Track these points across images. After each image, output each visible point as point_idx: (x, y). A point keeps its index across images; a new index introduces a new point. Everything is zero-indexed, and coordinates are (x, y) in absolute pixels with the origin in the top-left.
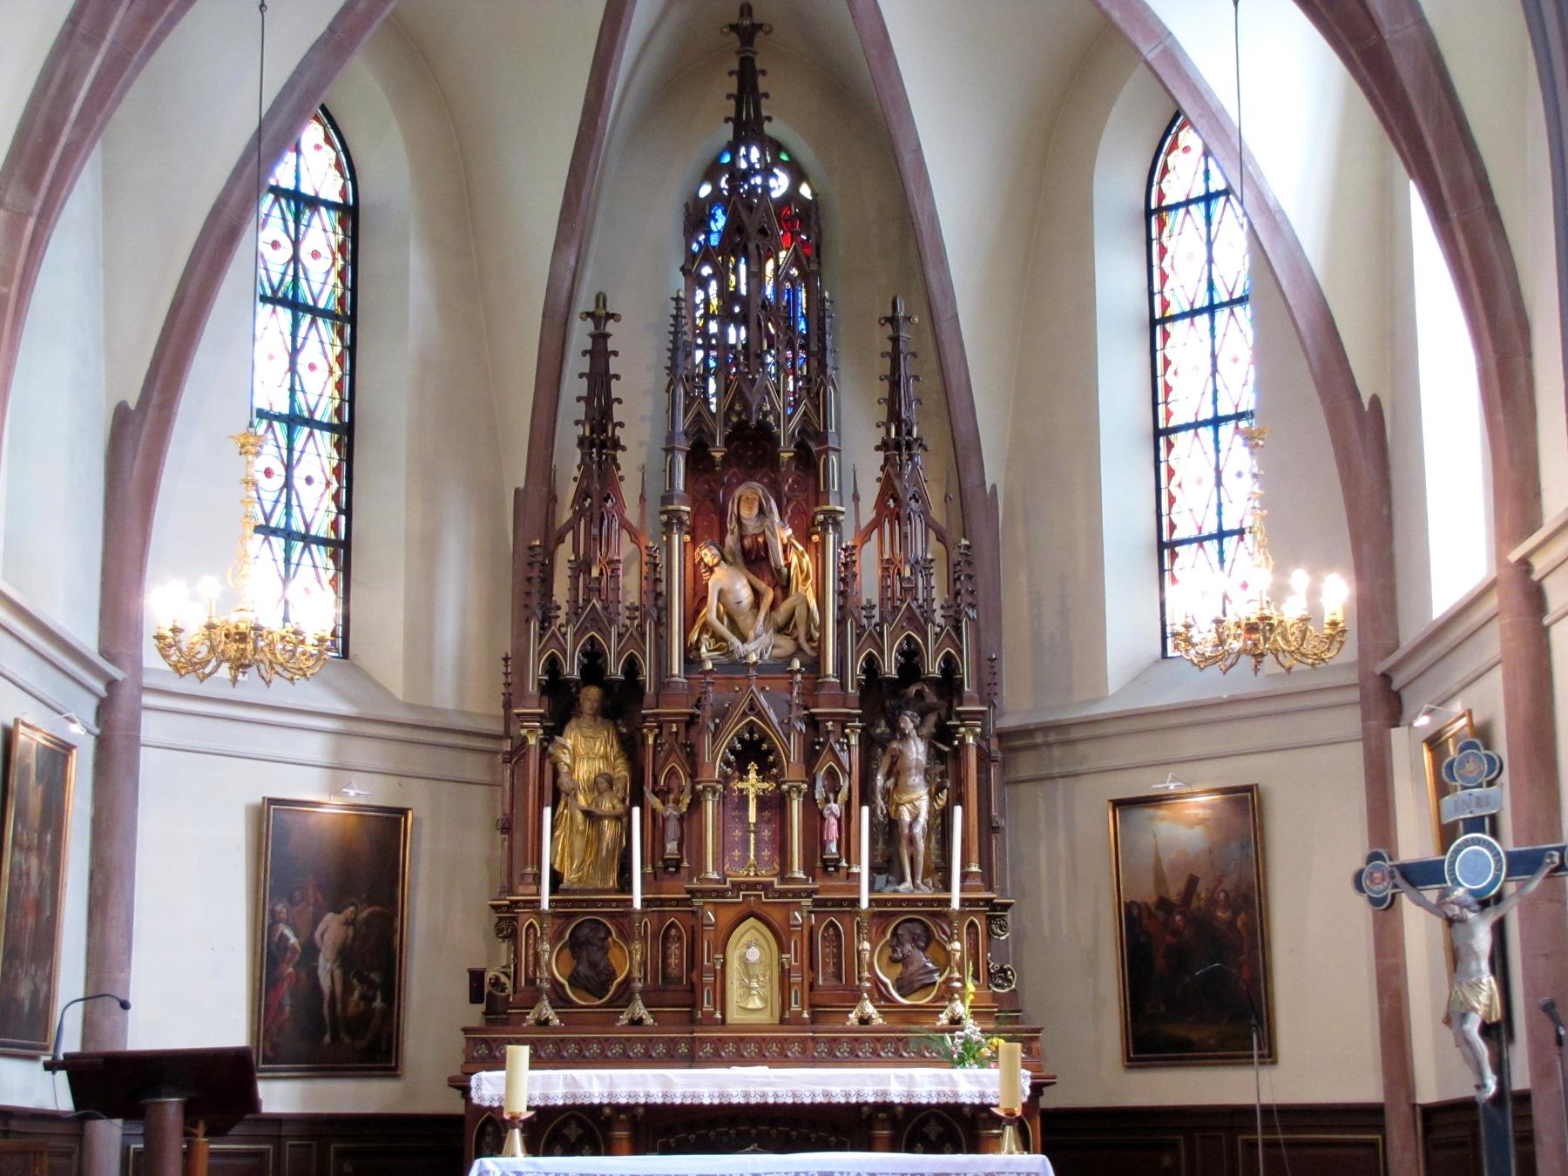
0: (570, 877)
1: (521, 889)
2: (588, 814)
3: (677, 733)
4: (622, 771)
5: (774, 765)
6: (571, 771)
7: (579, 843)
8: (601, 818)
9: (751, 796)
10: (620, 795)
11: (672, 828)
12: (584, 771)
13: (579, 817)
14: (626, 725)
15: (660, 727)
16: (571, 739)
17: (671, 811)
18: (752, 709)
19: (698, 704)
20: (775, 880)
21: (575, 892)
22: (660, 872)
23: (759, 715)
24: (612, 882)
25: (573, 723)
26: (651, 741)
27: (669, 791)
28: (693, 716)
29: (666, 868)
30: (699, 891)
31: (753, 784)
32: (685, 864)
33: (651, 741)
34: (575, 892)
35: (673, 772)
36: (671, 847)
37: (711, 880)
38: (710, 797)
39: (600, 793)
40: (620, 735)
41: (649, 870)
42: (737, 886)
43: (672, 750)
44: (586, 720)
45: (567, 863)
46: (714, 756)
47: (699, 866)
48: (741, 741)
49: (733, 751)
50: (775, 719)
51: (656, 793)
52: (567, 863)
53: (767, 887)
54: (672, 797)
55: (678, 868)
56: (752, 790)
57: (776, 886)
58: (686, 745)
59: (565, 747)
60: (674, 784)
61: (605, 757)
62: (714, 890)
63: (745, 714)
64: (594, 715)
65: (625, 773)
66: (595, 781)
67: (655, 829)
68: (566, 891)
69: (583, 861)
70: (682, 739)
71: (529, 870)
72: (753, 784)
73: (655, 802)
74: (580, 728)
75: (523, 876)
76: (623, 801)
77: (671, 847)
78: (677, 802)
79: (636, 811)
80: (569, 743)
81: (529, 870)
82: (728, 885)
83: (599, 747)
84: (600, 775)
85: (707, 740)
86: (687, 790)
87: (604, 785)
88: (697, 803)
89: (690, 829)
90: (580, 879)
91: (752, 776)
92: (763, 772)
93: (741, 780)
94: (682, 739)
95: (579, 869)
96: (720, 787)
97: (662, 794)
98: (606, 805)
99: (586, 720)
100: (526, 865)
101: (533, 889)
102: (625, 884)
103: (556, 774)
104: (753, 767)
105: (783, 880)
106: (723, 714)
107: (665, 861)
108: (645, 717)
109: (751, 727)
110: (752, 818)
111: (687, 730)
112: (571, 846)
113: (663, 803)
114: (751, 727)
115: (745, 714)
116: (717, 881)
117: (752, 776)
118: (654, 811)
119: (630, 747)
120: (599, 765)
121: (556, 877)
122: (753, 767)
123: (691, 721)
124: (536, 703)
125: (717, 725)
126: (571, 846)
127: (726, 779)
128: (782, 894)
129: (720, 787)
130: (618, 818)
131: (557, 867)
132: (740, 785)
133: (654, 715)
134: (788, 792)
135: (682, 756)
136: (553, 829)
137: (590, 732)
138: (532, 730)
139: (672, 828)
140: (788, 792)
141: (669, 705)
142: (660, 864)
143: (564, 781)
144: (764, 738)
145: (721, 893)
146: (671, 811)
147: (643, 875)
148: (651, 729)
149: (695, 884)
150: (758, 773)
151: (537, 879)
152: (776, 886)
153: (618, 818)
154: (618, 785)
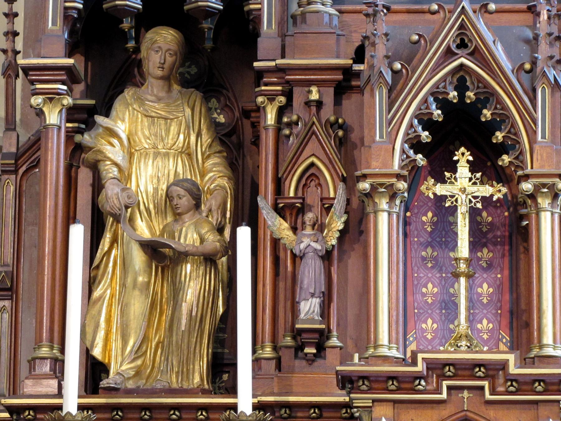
0: (120, 367)
1: (29, 386)
2: (153, 249)
3: (319, 104)
4: (215, 177)
5: (503, 149)
6: (124, 176)
7: (138, 306)
8: (181, 257)
9: (462, 210)
10: (214, 219)
11: (311, 273)
12: (149, 179)
13: (138, 258)
14: (225, 108)
15: (289, 95)
16: (126, 121)
17: (307, 242)
18: (462, 45)
19: (359, 55)
20: (511, 358)
21: (129, 393)
22: (287, 356)
23: (475, 54)
24: (198, 375)
25: (129, 93)
26: (271, 117)
27: (302, 210)
28: (347, 71)
29: (299, 348)
30: (364, 377)
31: (464, 186)
32: (334, 341)
33: (271, 117)
34: (129, 393)
35: (311, 175)
36: (309, 307)
37: (385, 359)
38: (383, 204)
39: (178, 216)
40: (215, 125)
41: (268, 352)
42: (437, 368)
43: (310, 133)
44: (153, 87)
45: (116, 345)
46: (390, 138)
47: (364, 338)
48: (443, 104)
49: (428, 123)
50: (507, 66)
51: (280, 211)
52: (116, 345)
53: (493, 370)
54: (309, 216)
55: (321, 348)
56: (462, 198)
57: (513, 370)
58: (334, 125)
59: (112, 133)
60: (313, 196)
61: (187, 153)
62: (392, 377)
63: (449, 54)
64: (167, 79)
65: (224, 182)
66: (169, 196)
67: (278, 264)
68: (112, 391)
69: (145, 339)
70: (328, 113)
71: (45, 351)
72: (464, 186)
73: (281, 227)
74: (141, 101)
75: (32, 362)
76: (220, 230)
77: (309, 307)
78: (320, 227)
79: (244, 234)
80: (122, 128)
81: (45, 351)
82: (420, 367)
83: (175, 135)
84: (177, 183)
85: (379, 97)
86: (339, 205)
87: (185, 201)
88: (357, 230)
89: (343, 275)
90: (138, 373)
91: (463, 171)
92: (486, 165)
93: (441, 180)
94: (328, 113)
95: (139, 353)
96: (402, 185)
97: (293, 212)
98: (191, 235)
99: (153, 87)
100: (38, 345)
101: (52, 385)
102: (222, 368)
103: (98, 186)
104: (463, 157)
105: (524, 362)
106: (411, 54)
107: (297, 334)
108: (260, 74)
109: (461, 79)
110: (463, 249)
111: (338, 102)
112: (123, 313)
113: (294, 229)
114: (461, 79)
115: (449, 54)
116: (403, 361)
117: (463, 171)
118: (276, 242)
119: (235, 143)
120: (176, 167)
121: (94, 372)
122: (463, 157)
123: (346, 83)
124: (61, 47)
125: (395, 73)
126: (123, 313)
127: (414, 175)
128: (524, 384)
129: (402, 185)
130: (209, 260)
131: (97, 352)
132: (441, 190)
133: (280, 70)
134: (532, 197)
135: (330, 147)
136: (91, 284)
137: (158, 109)
138: (52, 97)
139: (311, 273)
140: (532, 197)
141: (304, 53)
142: (289, 341)
143: (112, 193)
144: (487, 97)
145: (406, 382)
146: (307, 242)
147: (256, 362)
148: (271, 98)
149: (356, 366)
150: (473, 167)
151: (58, 368)
152: (513, 370)
153: (209, 260)
154: (210, 202)
